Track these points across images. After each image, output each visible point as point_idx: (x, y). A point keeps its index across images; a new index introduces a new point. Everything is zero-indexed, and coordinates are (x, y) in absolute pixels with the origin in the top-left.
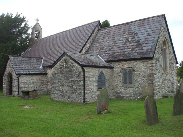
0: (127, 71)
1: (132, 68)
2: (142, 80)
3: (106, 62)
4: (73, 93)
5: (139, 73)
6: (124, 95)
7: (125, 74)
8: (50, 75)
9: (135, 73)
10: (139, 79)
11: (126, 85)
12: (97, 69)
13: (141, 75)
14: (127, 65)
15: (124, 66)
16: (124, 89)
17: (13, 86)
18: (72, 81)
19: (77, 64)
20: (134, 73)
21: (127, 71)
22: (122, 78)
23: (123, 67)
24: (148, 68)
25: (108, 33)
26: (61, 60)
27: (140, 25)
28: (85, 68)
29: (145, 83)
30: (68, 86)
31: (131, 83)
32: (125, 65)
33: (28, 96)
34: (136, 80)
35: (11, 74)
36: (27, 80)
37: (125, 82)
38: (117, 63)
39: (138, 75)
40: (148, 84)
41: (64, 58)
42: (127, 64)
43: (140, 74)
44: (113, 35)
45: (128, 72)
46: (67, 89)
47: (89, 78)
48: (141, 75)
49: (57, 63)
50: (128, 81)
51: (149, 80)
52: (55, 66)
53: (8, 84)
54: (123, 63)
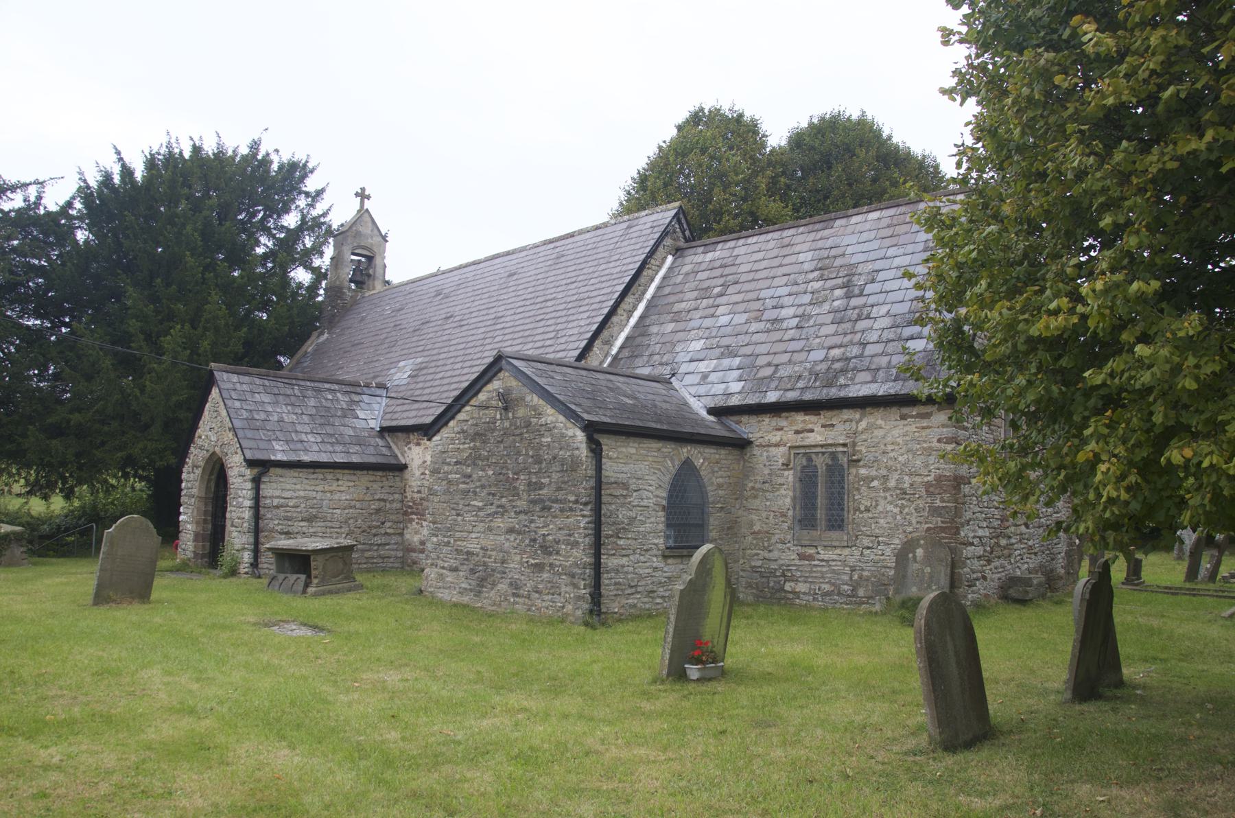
0: (820, 462)
1: (844, 445)
2: (897, 510)
3: (711, 411)
4: (539, 567)
5: (883, 472)
6: (802, 587)
7: (807, 479)
8: (417, 473)
9: (863, 471)
10: (882, 502)
11: (814, 533)
12: (668, 448)
13: (892, 484)
14: (819, 432)
15: (806, 434)
16: (802, 557)
17: (228, 523)
18: (533, 502)
19: (561, 418)
20: (853, 471)
21: (820, 462)
22: (794, 499)
23: (798, 440)
24: (928, 451)
25: (723, 266)
26: (482, 396)
27: (888, 232)
28: (606, 441)
29: (910, 524)
30: (511, 531)
31: (836, 523)
32: (812, 431)
33: (303, 577)
34: (867, 510)
35: (220, 459)
36: (302, 493)
37: (806, 520)
38: (767, 421)
39: (875, 483)
40: (929, 529)
41: (496, 385)
42: (818, 428)
43: (885, 478)
44: (751, 276)
45: (822, 469)
46: (509, 542)
47: (625, 492)
48: (892, 484)
49: (459, 411)
50: (820, 514)
51: (935, 511)
52: (451, 424)
53: (205, 513)
54: (800, 419)
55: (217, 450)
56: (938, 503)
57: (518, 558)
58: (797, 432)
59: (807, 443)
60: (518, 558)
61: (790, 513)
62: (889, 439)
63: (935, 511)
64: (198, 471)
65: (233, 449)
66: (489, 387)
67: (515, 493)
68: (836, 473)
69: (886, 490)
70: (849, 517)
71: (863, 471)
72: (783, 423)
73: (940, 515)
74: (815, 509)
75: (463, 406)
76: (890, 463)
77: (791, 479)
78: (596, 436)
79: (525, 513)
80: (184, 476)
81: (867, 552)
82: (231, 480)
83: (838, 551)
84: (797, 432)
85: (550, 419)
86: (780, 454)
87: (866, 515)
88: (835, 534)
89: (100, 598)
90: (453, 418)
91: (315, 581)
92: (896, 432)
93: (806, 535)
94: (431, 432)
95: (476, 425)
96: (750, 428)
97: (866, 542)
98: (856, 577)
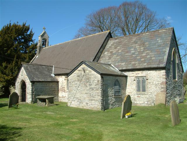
0: (141, 79)
1: (145, 76)
2: (155, 88)
3: (120, 71)
4: (92, 100)
5: (153, 81)
6: (138, 102)
7: (138, 83)
8: (61, 83)
9: (149, 81)
10: (152, 87)
11: (140, 92)
12: (114, 77)
13: (154, 83)
14: (140, 74)
15: (138, 74)
16: (138, 97)
17: (26, 93)
18: (90, 88)
19: (95, 73)
20: (147, 81)
21: (141, 79)
22: (136, 86)
23: (136, 76)
24: (160, 77)
25: (119, 43)
26: (79, 69)
27: (150, 37)
28: (103, 76)
29: (158, 90)
30: (86, 93)
31: (144, 90)
32: (139, 74)
33: (45, 103)
34: (150, 88)
35: (24, 81)
36: (40, 87)
37: (138, 90)
38: (131, 73)
39: (151, 83)
40: (161, 91)
41: (82, 66)
42: (140, 73)
43: (153, 82)
44: (125, 45)
45: (141, 81)
46: (85, 96)
47: (107, 86)
48: (154, 83)
49: (74, 71)
50: (141, 89)
51: (162, 88)
52: (73, 74)
53: (21, 91)
54: (137, 72)
55: (23, 79)
56: (163, 86)
57: (87, 98)
58: (136, 74)
59: (138, 76)
60: (87, 98)
61: (135, 89)
62: (153, 75)
63: (162, 88)
64: (19, 83)
65: (27, 79)
66: (80, 67)
67: (87, 86)
68: (144, 82)
69: (153, 84)
70: (146, 89)
71: (149, 81)
72: (133, 72)
73: (163, 89)
74: (140, 88)
75: (75, 70)
76: (154, 79)
77: (135, 83)
78: (103, 76)
79: (89, 90)
80: (16, 84)
81: (150, 95)
82: (27, 85)
83: (145, 95)
84: (136, 74)
85: (93, 73)
86: (133, 78)
87: (149, 89)
88: (143, 92)
89: (9, 108)
90: (73, 73)
91: (47, 104)
92: (155, 74)
93: (139, 93)
94: (69, 75)
95: (78, 74)
96: (126, 74)
97: (150, 94)
98: (148, 100)
